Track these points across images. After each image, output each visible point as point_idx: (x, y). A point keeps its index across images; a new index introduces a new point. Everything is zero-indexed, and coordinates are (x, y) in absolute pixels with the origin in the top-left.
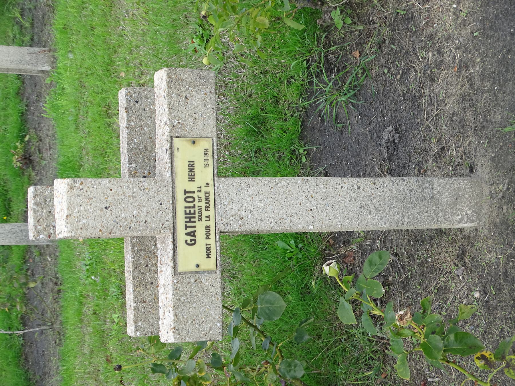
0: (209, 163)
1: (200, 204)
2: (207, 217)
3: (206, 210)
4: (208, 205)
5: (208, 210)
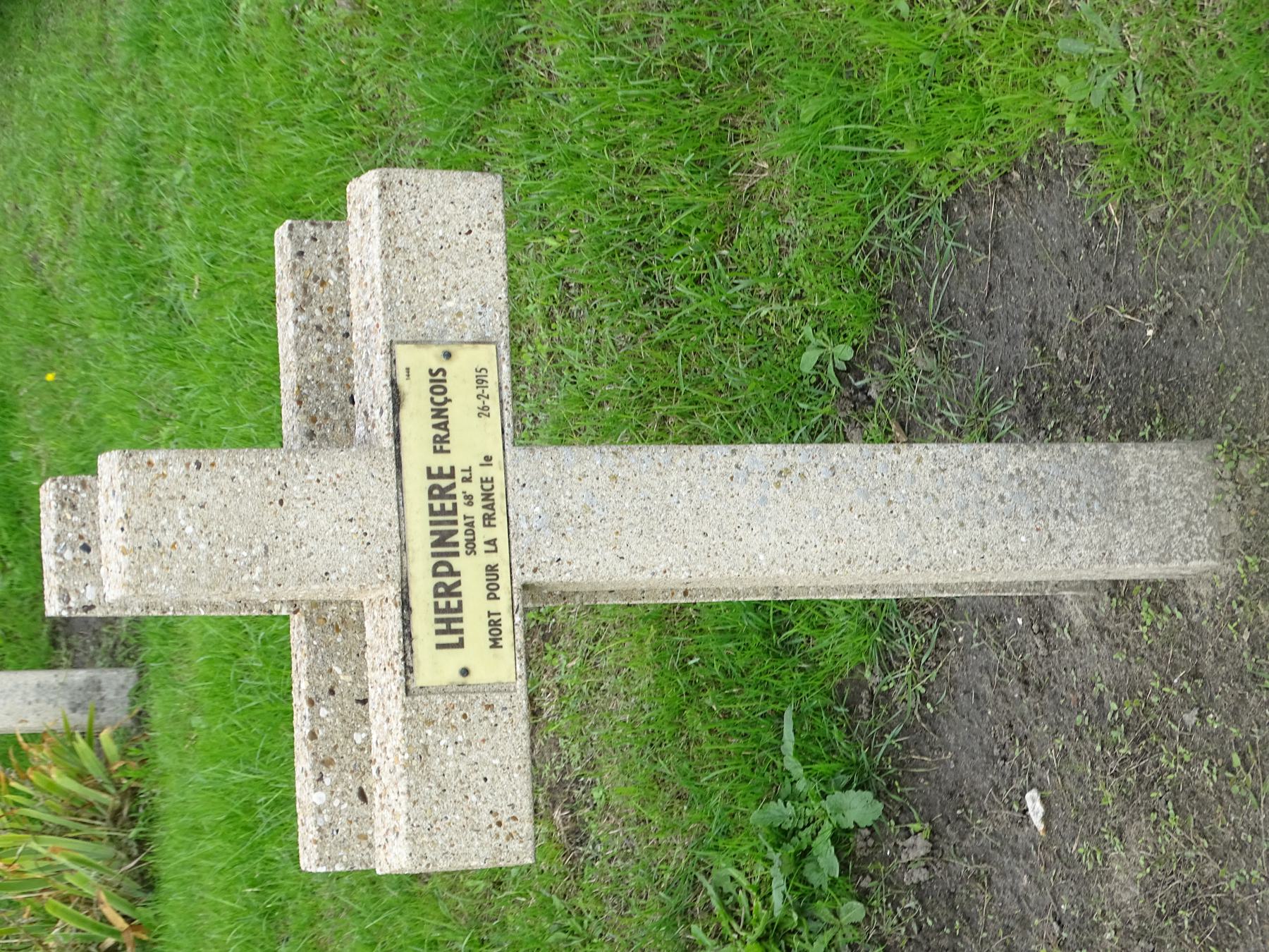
0: (488, 403)
1: (469, 511)
2: (488, 543)
3: (485, 525)
4: (490, 512)
5: (490, 525)
